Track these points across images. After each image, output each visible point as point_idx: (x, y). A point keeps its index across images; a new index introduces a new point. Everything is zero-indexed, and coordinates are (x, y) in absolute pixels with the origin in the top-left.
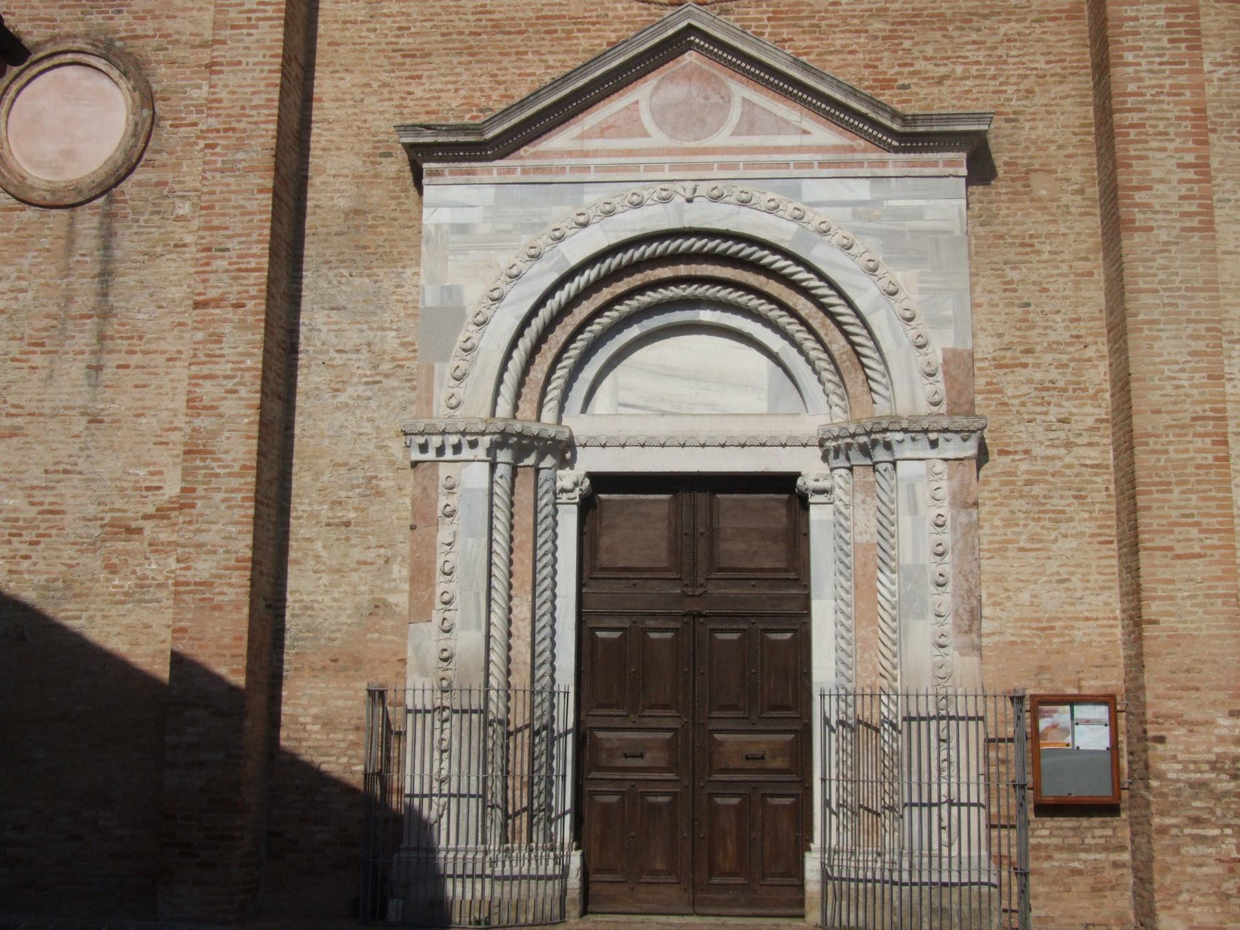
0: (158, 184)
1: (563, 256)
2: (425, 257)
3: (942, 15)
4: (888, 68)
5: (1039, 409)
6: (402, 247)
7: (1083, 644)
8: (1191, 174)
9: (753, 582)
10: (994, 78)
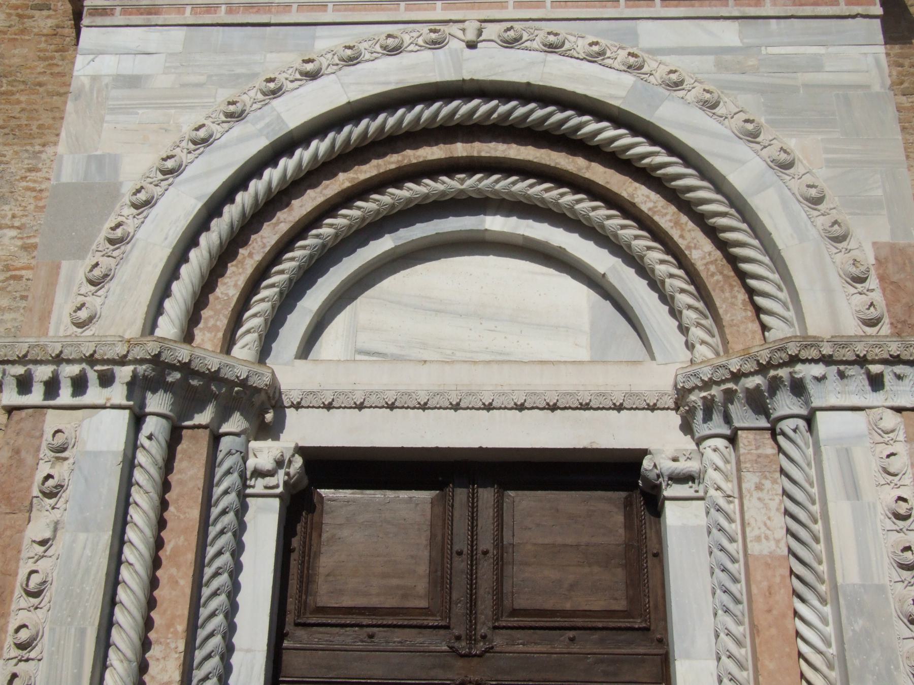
1: (279, 116)
6: (46, 118)
9: (571, 634)
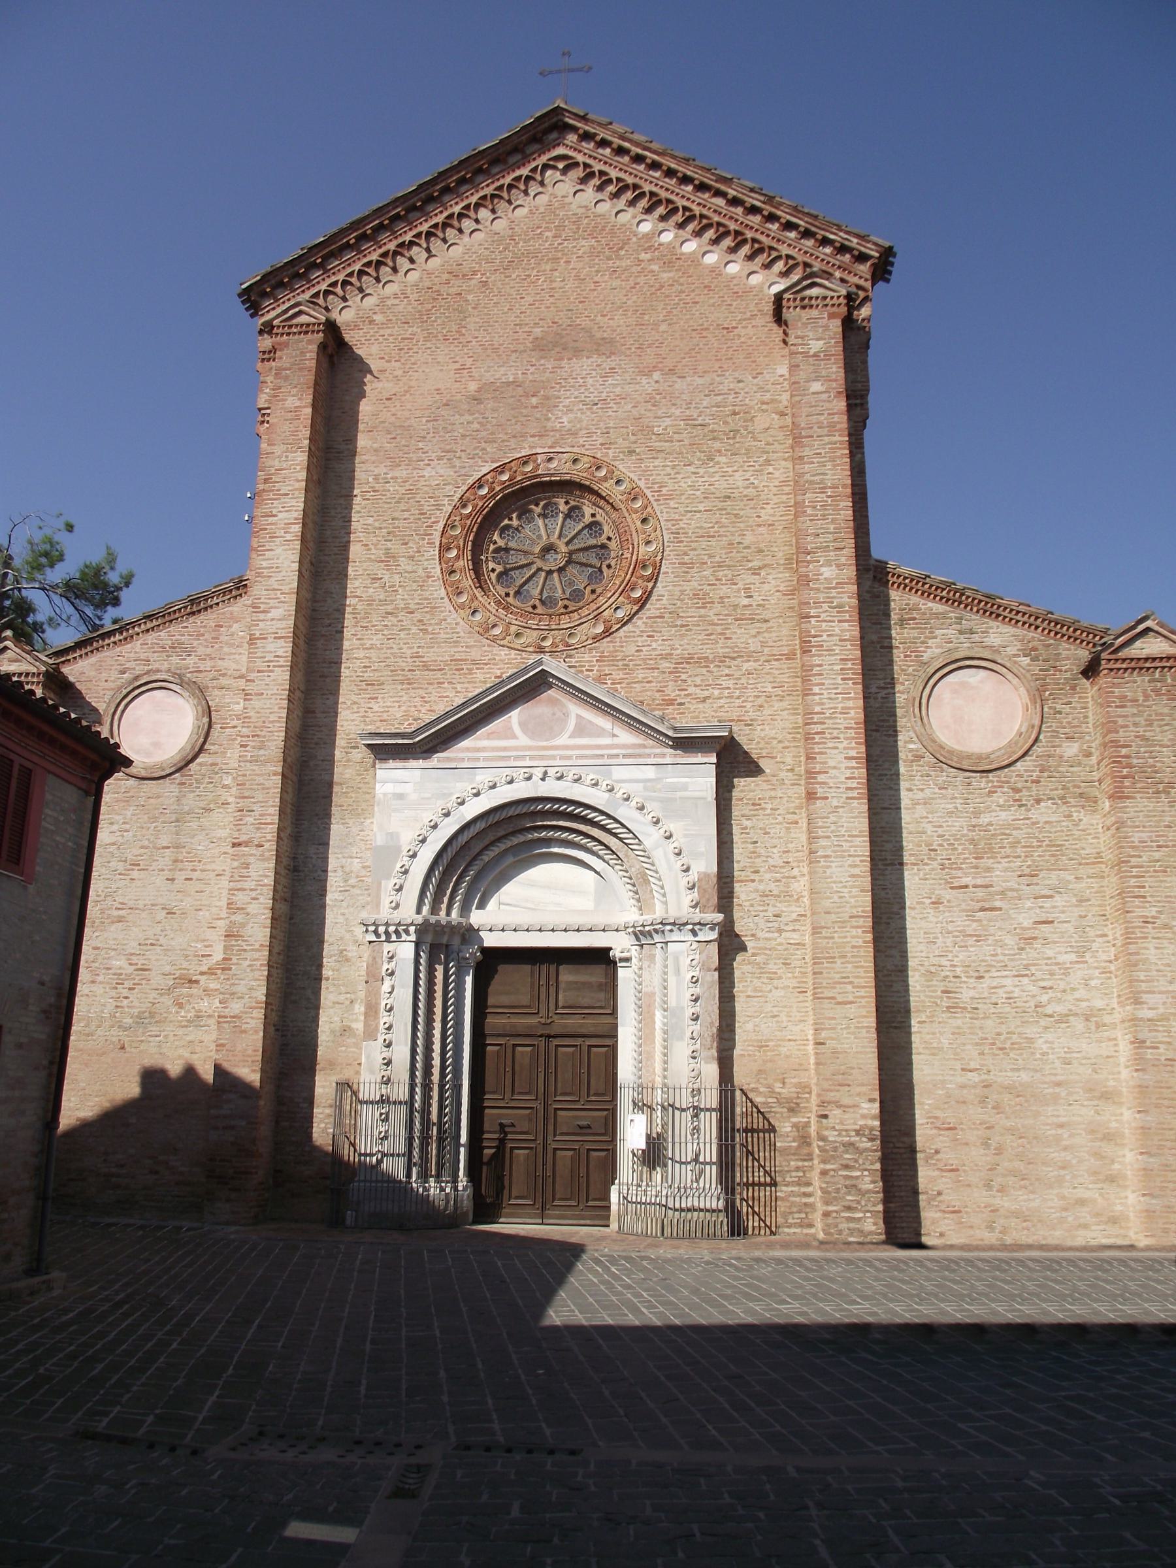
0: (212, 765)
2: (377, 814)
3: (707, 657)
4: (671, 691)
5: (761, 908)
6: (364, 805)
7: (787, 1057)
10: (738, 698)
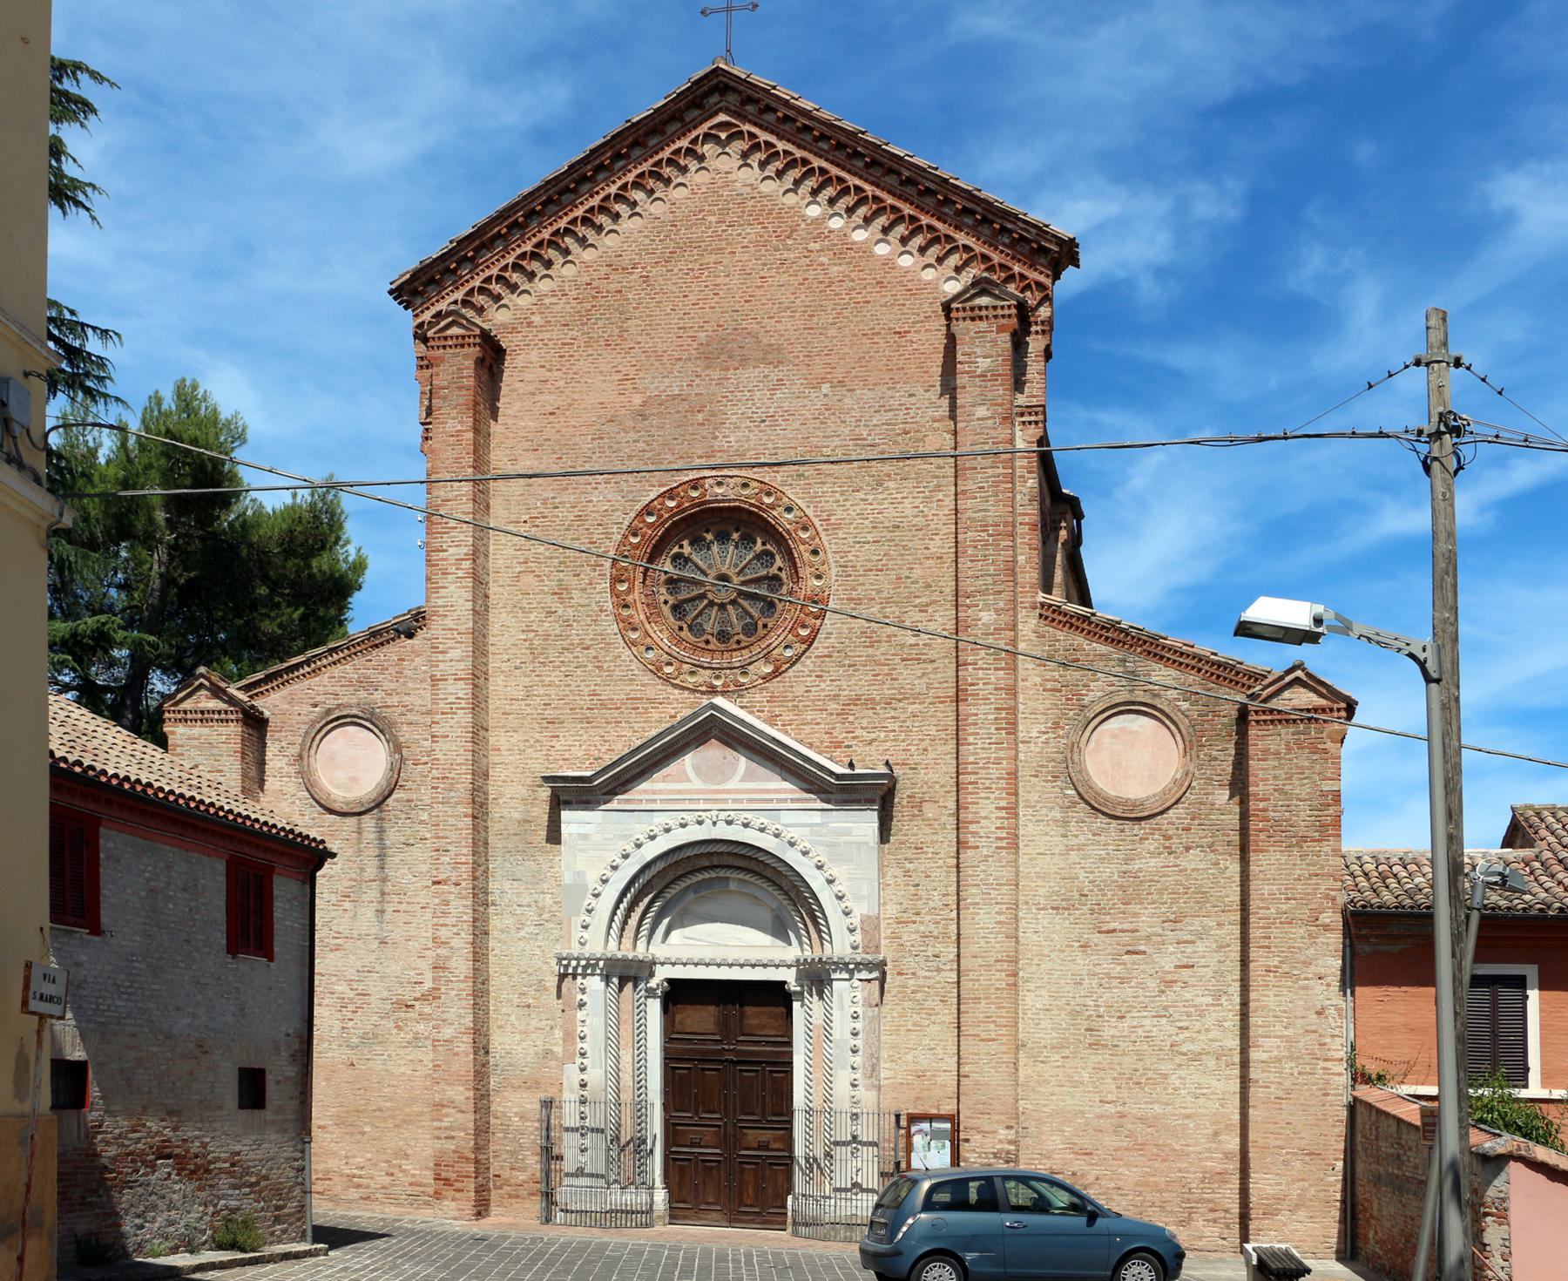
8: (1003, 814)
